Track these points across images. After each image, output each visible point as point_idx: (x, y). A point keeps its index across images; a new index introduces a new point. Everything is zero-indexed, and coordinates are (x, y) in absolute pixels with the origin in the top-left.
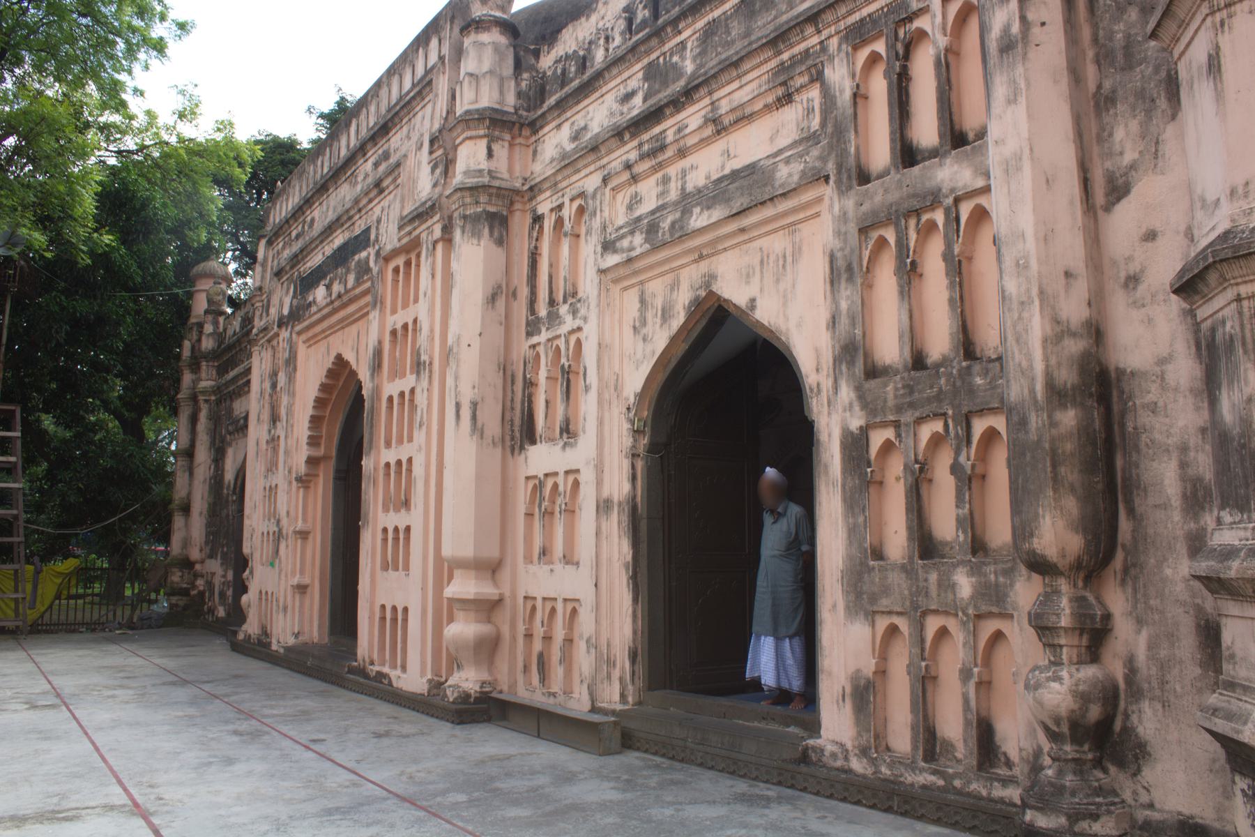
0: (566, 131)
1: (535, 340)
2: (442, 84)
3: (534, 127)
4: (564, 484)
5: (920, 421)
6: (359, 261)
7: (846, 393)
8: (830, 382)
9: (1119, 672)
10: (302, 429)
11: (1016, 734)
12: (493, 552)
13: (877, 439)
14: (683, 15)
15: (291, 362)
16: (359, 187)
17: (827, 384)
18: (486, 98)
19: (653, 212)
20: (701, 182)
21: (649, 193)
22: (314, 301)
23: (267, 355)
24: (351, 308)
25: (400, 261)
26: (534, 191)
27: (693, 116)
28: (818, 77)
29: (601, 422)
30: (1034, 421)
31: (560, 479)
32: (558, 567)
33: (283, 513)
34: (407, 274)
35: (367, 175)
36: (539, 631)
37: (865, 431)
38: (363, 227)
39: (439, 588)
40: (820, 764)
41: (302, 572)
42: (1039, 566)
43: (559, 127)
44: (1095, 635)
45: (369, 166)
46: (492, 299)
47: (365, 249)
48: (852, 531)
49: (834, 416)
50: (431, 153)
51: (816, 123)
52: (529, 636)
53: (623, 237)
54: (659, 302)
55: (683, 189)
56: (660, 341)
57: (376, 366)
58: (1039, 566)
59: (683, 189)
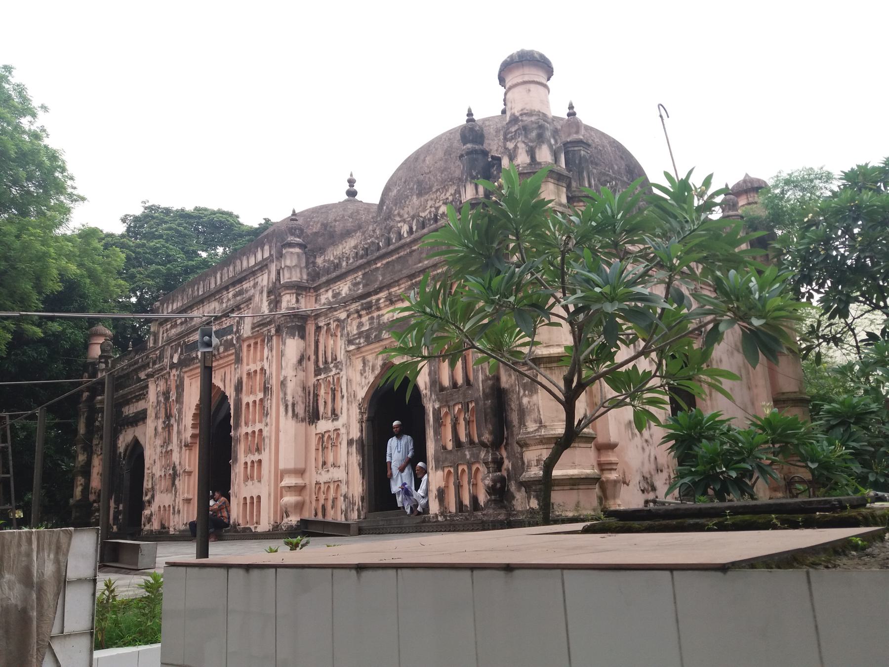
0: (330, 294)
1: (319, 377)
2: (273, 268)
3: (317, 289)
4: (333, 436)
5: (454, 405)
9: (505, 474)
10: (188, 419)
11: (482, 498)
12: (301, 466)
13: (444, 410)
15: (180, 387)
16: (224, 305)
17: (429, 393)
18: (296, 277)
20: (386, 321)
23: (162, 383)
25: (252, 342)
26: (317, 316)
29: (348, 410)
30: (481, 403)
31: (331, 434)
32: (331, 469)
33: (177, 463)
34: (255, 348)
35: (229, 300)
36: (322, 497)
37: (439, 408)
39: (276, 485)
40: (429, 521)
41: (188, 493)
42: (483, 445)
43: (327, 291)
44: (498, 464)
45: (230, 295)
46: (300, 361)
49: (430, 406)
50: (268, 297)
52: (317, 500)
53: (356, 339)
54: (371, 364)
56: (371, 379)
57: (239, 388)
58: (483, 445)
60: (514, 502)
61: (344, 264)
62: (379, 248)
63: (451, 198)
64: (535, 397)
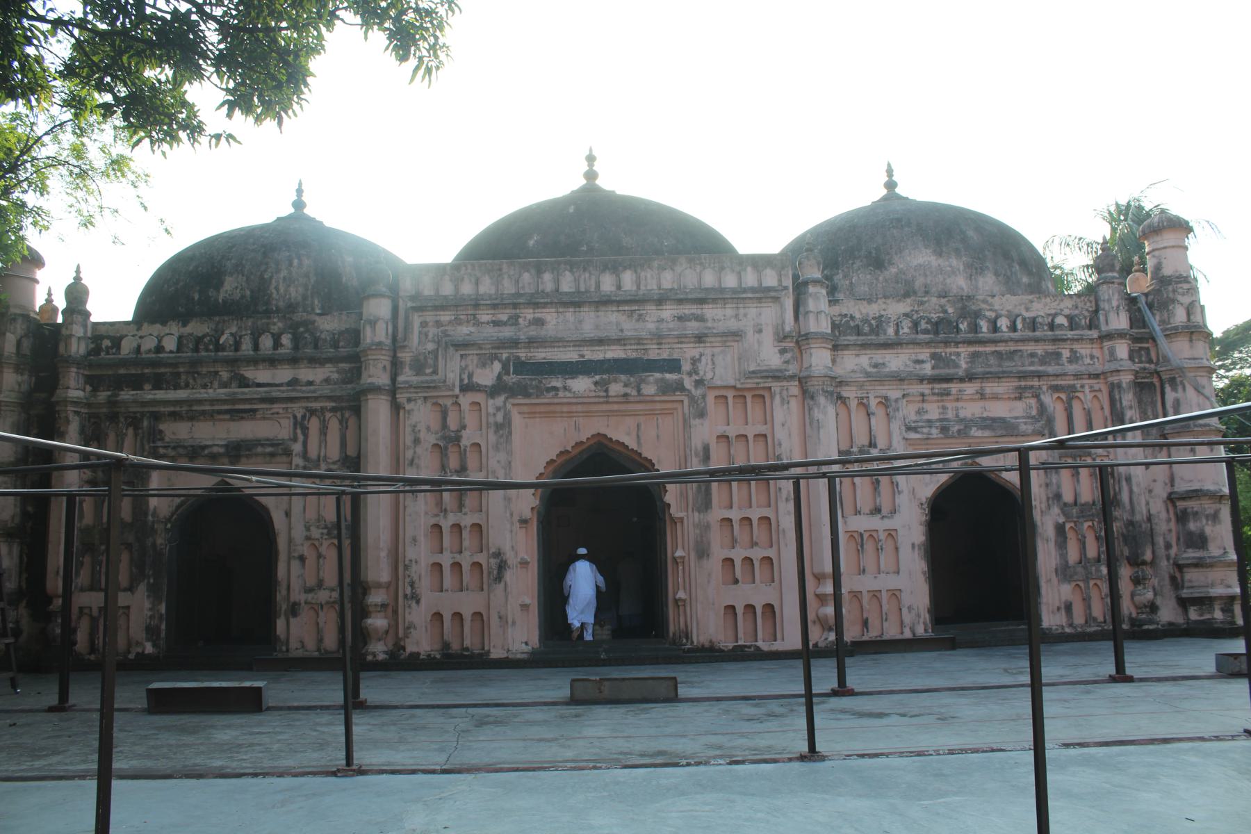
6: (662, 380)
7: (1056, 510)
8: (1044, 506)
13: (1068, 526)
14: (964, 342)
16: (651, 326)
19: (941, 420)
20: (969, 416)
21: (933, 412)
27: (970, 388)
28: (1037, 396)
33: (507, 548)
38: (665, 356)
43: (857, 355)
48: (1061, 555)
51: (1034, 412)
55: (957, 416)
56: (944, 478)
59: (957, 416)
62: (958, 330)
63: (1067, 312)
64: (1218, 527)
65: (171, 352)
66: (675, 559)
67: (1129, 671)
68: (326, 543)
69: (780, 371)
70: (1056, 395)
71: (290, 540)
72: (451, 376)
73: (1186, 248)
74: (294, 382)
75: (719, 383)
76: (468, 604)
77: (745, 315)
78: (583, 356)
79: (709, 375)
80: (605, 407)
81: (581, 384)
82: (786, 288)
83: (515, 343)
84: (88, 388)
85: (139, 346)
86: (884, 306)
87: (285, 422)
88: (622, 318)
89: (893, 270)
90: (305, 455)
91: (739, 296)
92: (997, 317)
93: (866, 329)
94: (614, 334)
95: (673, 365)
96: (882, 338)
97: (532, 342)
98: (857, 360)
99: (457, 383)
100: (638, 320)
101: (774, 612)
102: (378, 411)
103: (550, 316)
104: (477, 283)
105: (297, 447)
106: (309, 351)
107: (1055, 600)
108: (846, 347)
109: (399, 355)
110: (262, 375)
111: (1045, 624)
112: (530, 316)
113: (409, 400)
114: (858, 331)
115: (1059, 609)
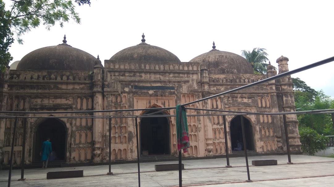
16: (167, 78)
22: (148, 93)
24: (164, 98)
33: (133, 131)
37: (261, 128)
38: (171, 86)
47: (172, 89)
56: (233, 116)
60: (283, 149)
61: (221, 81)
65: (35, 79)
66: (173, 135)
67: (292, 162)
68: (82, 132)
69: (197, 90)
70: (258, 98)
71: (72, 131)
72: (118, 89)
73: (288, 64)
74: (73, 89)
75: (183, 92)
76: (123, 147)
77: (190, 77)
78: (151, 85)
79: (181, 91)
80: (156, 97)
81: (151, 92)
82: (199, 71)
83: (135, 81)
84: (9, 88)
85: (25, 78)
86: (219, 75)
87: (70, 100)
88: (161, 77)
89: (220, 67)
90: (76, 108)
91: (188, 73)
92: (245, 79)
93: (215, 81)
94: (159, 79)
95: (173, 88)
96: (219, 83)
97: (139, 82)
98: (213, 88)
99: (120, 91)
100: (164, 77)
101: (197, 148)
102: (99, 99)
103: (143, 75)
104: (125, 66)
105: (74, 106)
106: (78, 81)
107: (259, 145)
108: (211, 85)
109: (105, 83)
110: (64, 87)
111: (257, 151)
112: (139, 75)
113: (107, 94)
114: (214, 81)
115: (261, 148)
